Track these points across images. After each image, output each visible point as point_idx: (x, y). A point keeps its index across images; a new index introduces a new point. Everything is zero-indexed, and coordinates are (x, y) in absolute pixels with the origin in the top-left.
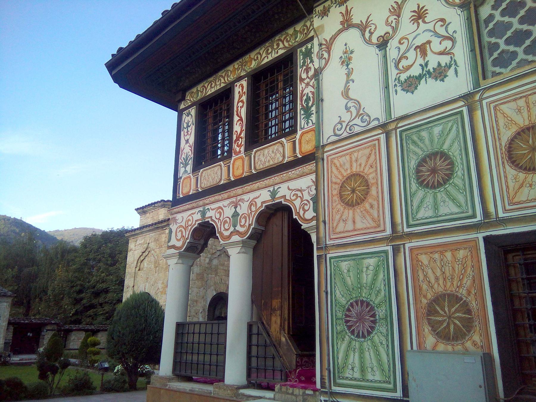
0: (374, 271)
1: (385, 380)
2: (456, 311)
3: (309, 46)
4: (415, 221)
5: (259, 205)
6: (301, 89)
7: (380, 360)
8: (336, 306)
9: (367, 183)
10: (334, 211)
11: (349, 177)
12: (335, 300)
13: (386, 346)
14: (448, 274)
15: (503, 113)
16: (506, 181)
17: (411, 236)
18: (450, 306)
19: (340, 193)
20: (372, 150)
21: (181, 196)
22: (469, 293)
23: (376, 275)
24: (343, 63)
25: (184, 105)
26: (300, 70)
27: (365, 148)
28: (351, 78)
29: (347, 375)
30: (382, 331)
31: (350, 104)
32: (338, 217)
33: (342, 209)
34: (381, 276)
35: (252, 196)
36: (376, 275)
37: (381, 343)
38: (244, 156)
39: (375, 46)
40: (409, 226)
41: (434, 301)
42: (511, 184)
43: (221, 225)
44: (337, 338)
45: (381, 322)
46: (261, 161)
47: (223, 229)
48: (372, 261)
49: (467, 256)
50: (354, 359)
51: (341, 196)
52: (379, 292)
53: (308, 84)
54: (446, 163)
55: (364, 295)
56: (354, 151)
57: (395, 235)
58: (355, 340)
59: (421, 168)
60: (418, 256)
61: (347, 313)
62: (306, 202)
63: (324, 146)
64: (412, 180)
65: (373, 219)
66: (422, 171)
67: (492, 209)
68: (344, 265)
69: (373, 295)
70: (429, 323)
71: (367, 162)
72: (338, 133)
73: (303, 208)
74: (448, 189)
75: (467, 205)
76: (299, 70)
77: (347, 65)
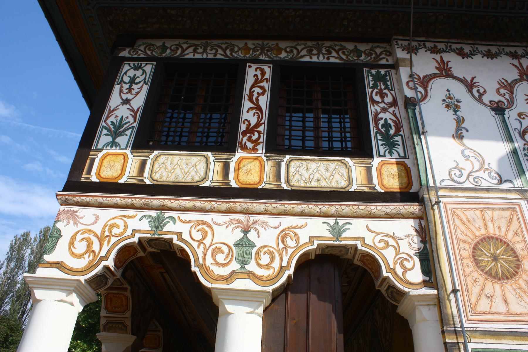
3: (383, 72)
5: (304, 239)
6: (373, 110)
9: (515, 252)
10: (469, 279)
11: (484, 238)
19: (474, 256)
20: (512, 215)
21: (94, 179)
24: (448, 106)
25: (129, 53)
26: (370, 90)
27: (503, 209)
28: (463, 126)
31: (467, 152)
32: (475, 290)
33: (481, 279)
35: (287, 222)
38: (265, 159)
39: (489, 108)
43: (205, 253)
46: (301, 175)
47: (209, 261)
51: (477, 262)
53: (384, 110)
56: (488, 209)
62: (406, 256)
63: (437, 189)
71: (509, 226)
72: (455, 178)
73: (402, 265)
76: (369, 91)
77: (456, 112)
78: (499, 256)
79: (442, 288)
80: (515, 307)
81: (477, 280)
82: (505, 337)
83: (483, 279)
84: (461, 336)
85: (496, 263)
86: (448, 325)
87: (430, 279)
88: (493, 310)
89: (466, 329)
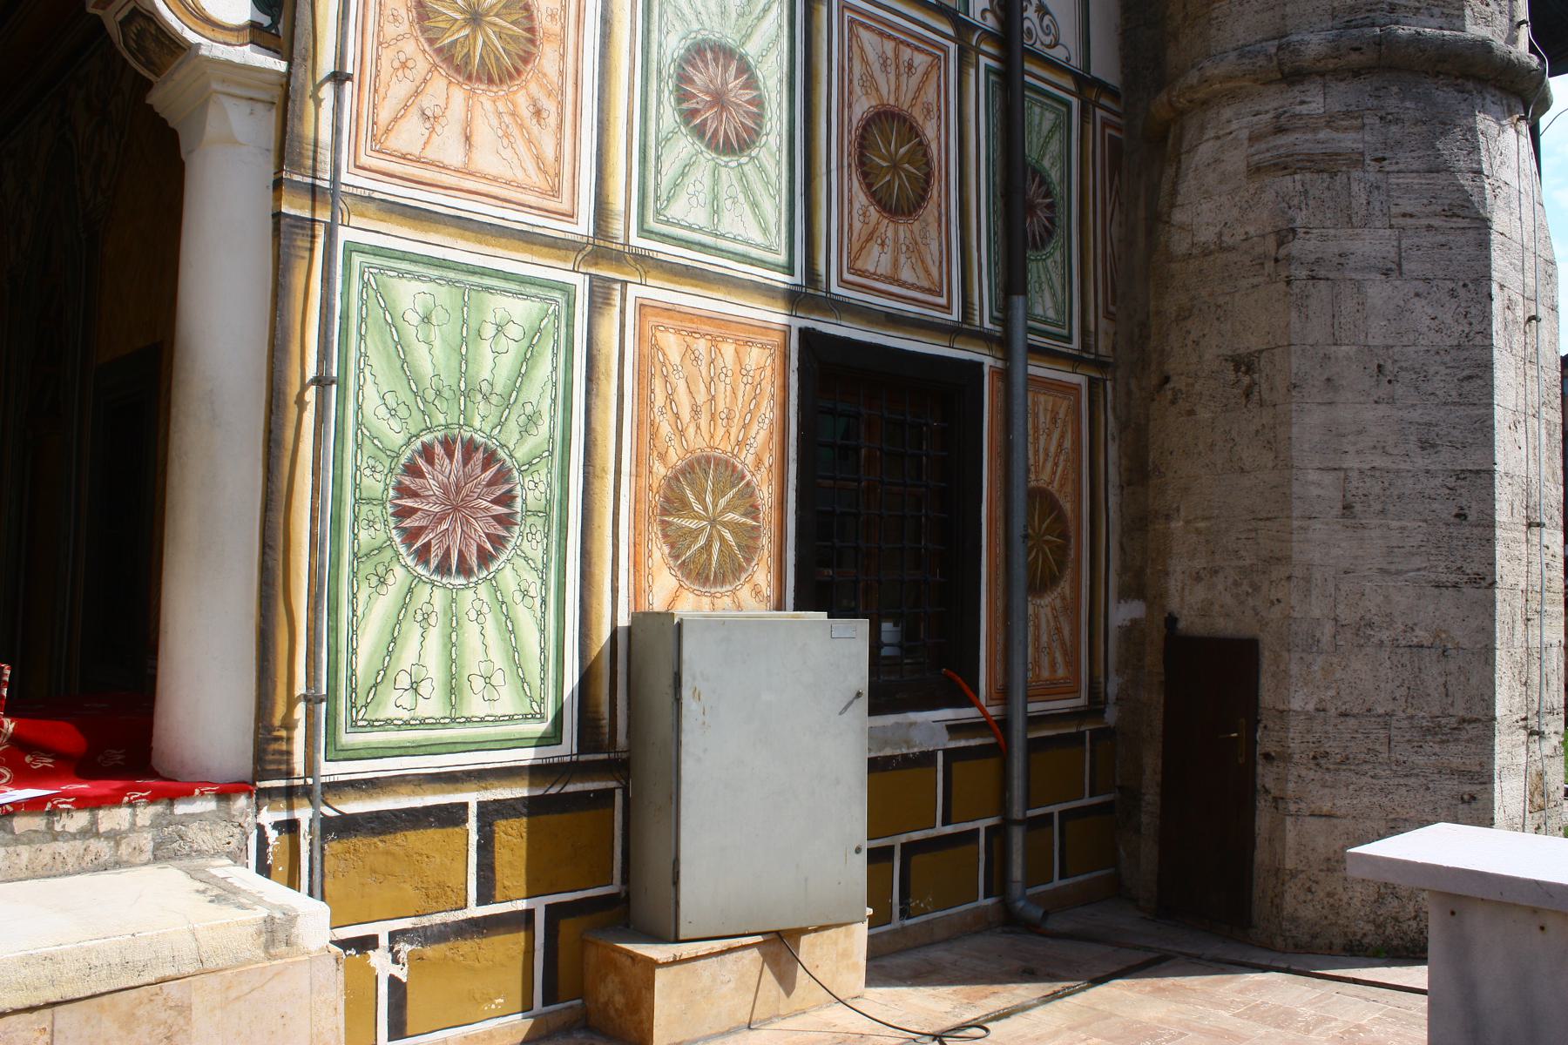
0: (525, 343)
1: (528, 710)
2: (730, 507)
4: (662, 222)
7: (515, 649)
8: (359, 446)
9: (530, 17)
10: (387, 55)
12: (359, 425)
13: (538, 601)
14: (721, 406)
15: (862, 49)
16: (850, 213)
17: (646, 263)
18: (718, 493)
22: (759, 461)
23: (528, 359)
29: (389, 712)
30: (530, 554)
32: (399, 90)
33: (422, 65)
34: (543, 368)
36: (528, 359)
37: (525, 593)
40: (644, 232)
41: (683, 472)
42: (857, 225)
44: (355, 574)
45: (530, 520)
48: (520, 311)
49: (764, 368)
50: (423, 652)
52: (532, 420)
54: (749, 94)
55: (477, 424)
57: (602, 243)
58: (433, 583)
59: (690, 69)
60: (658, 334)
61: (407, 481)
64: (666, 93)
65: (538, 159)
66: (691, 81)
67: (822, 269)
68: (409, 295)
69: (513, 426)
70: (665, 536)
74: (746, 168)
75: (779, 232)
78: (487, 15)
79: (305, 60)
80: (486, 160)
81: (411, 64)
82: (441, 227)
83: (427, 66)
84: (325, 203)
85: (474, 31)
86: (297, 166)
87: (274, 24)
88: (430, 154)
89: (343, 188)
